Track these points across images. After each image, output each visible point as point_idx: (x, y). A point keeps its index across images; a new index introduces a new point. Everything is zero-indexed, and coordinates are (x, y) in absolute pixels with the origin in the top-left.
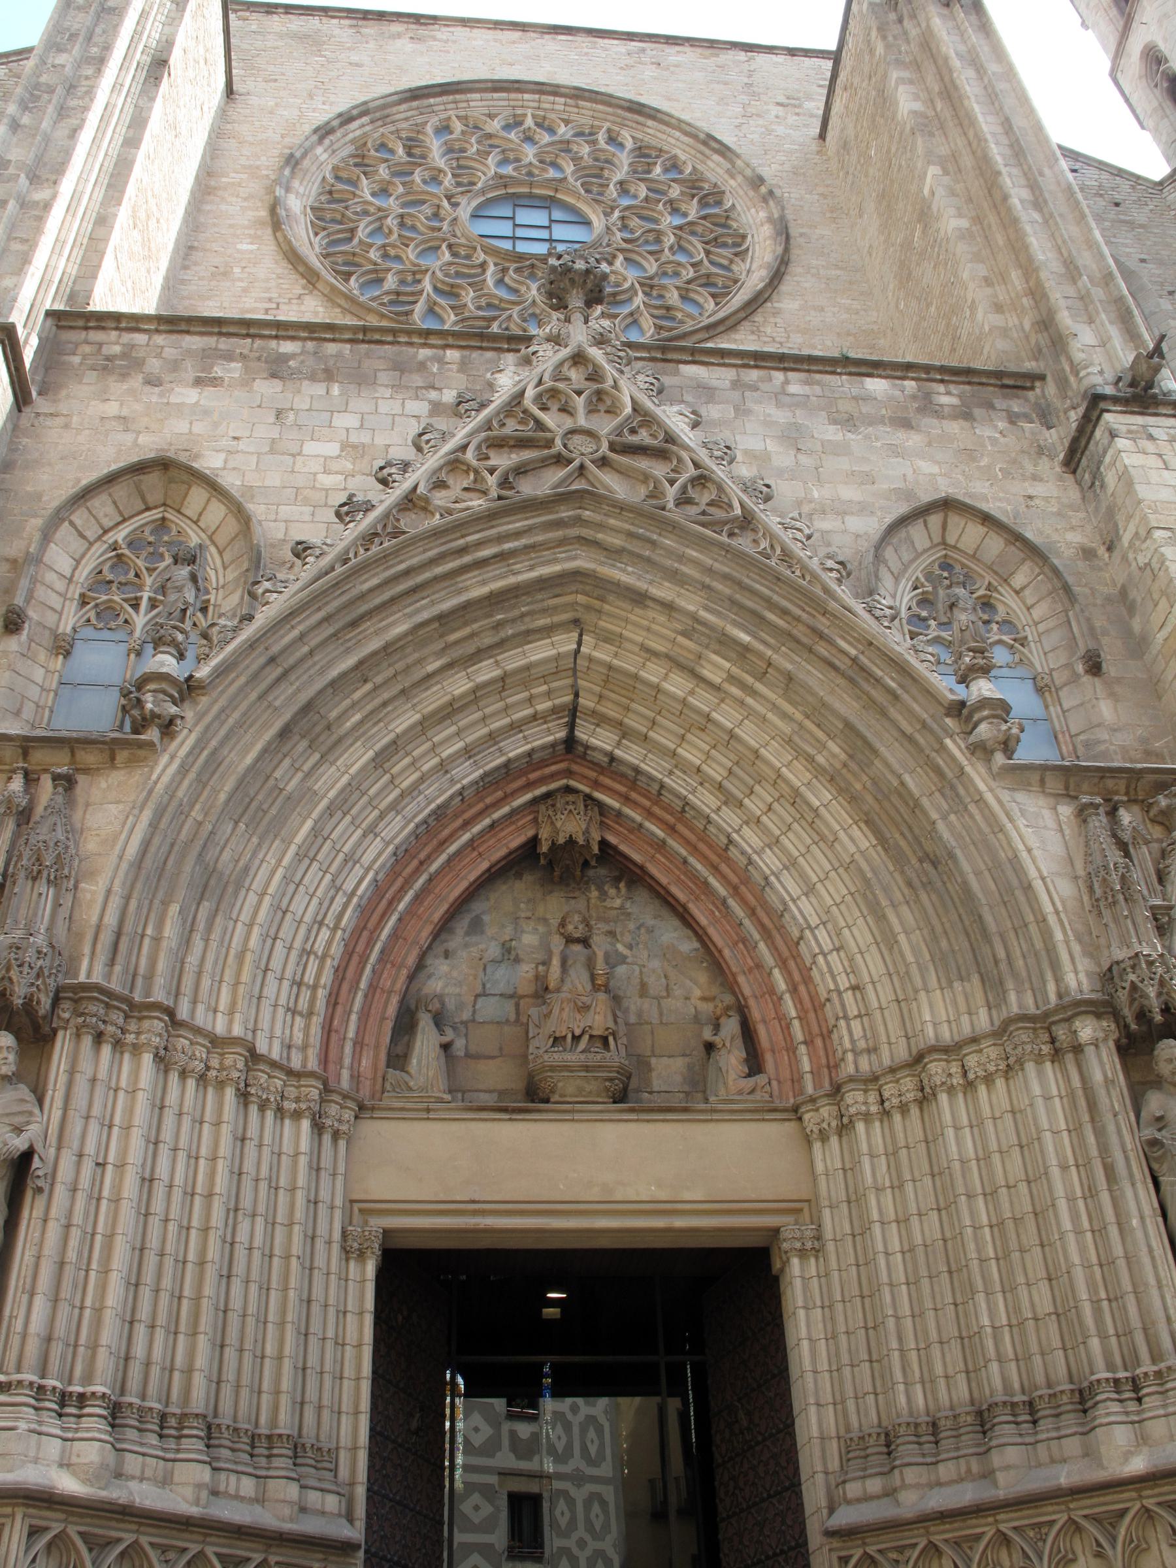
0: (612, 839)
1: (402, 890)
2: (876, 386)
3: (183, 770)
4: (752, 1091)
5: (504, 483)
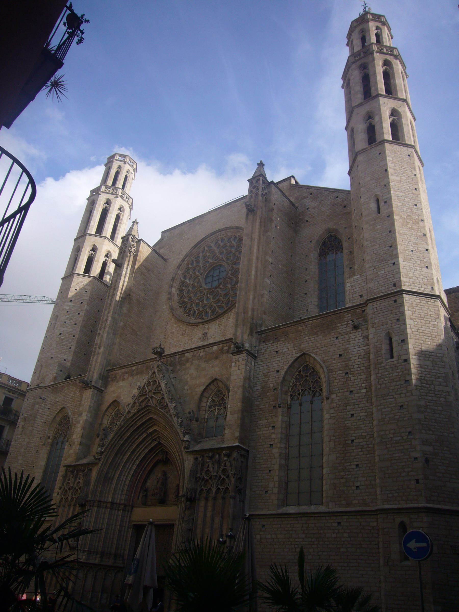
0: (168, 457)
1: (141, 471)
2: (215, 348)
3: (102, 464)
4: (175, 501)
5: (140, 405)
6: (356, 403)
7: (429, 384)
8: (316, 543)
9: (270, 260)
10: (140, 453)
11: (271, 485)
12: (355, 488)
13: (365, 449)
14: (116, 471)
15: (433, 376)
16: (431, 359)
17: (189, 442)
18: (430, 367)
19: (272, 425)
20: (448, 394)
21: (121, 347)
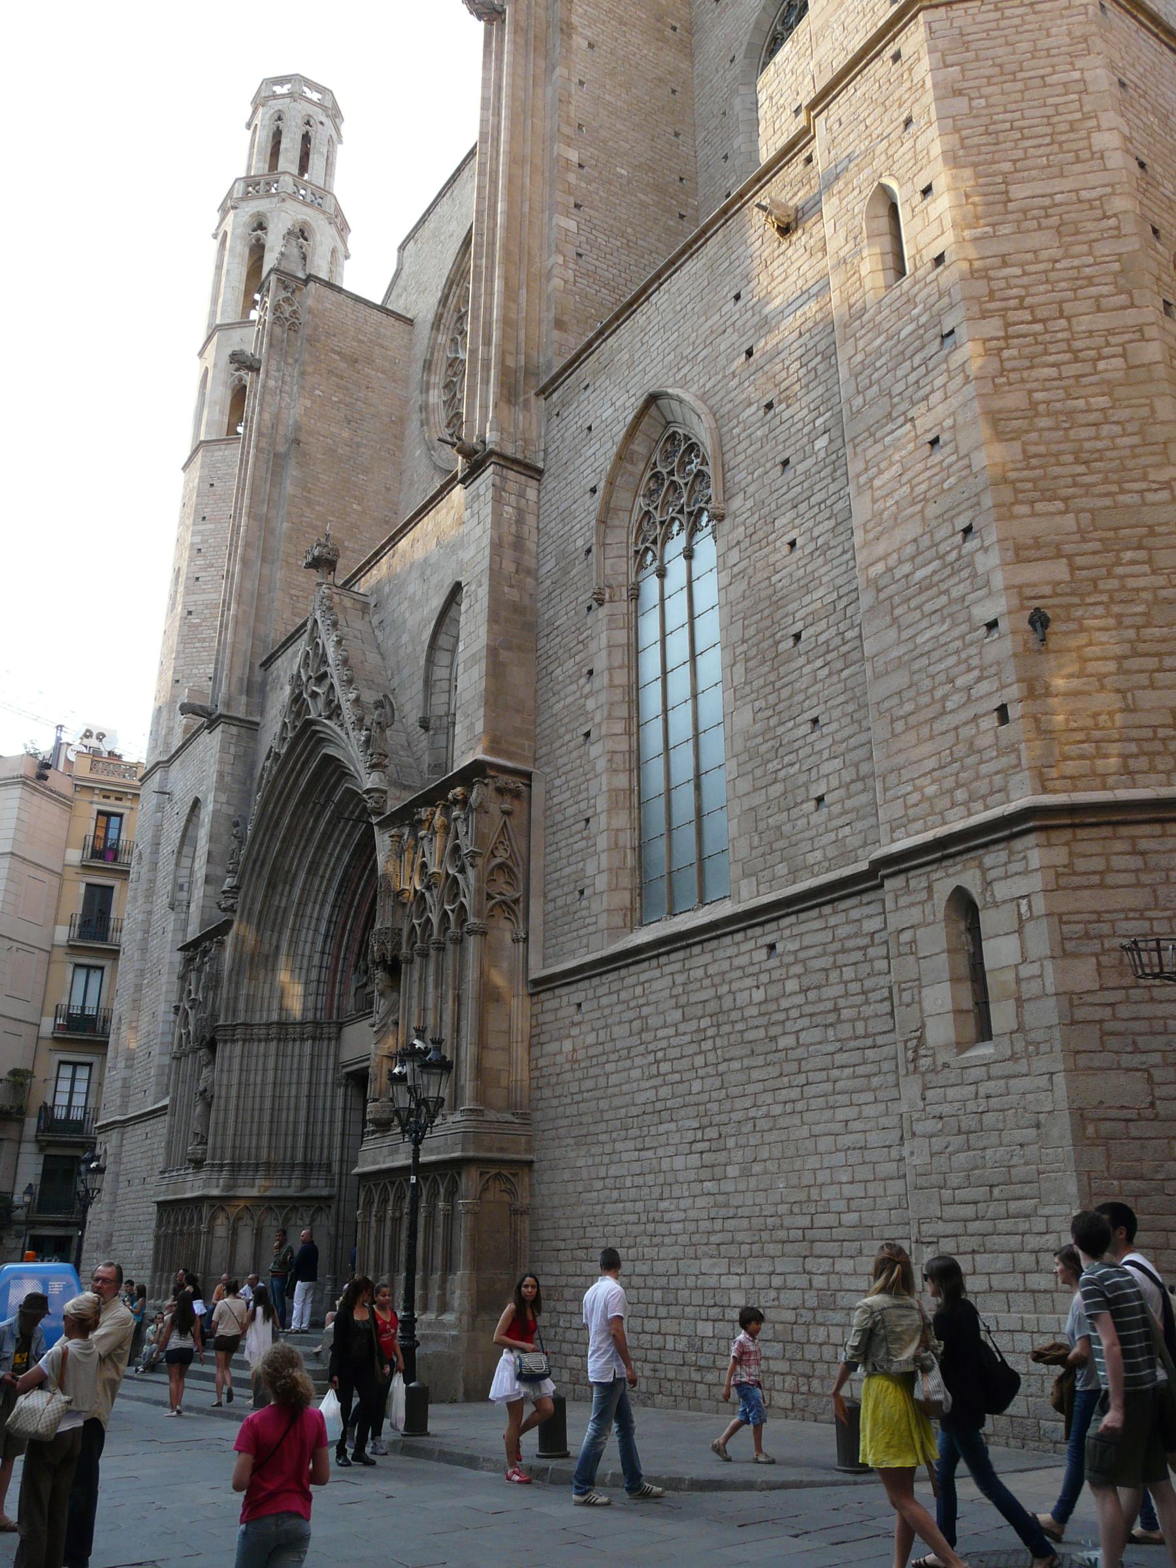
6: (801, 498)
7: (1043, 321)
8: (710, 1032)
9: (574, 156)
10: (334, 869)
11: (591, 869)
12: (812, 804)
13: (834, 654)
14: (280, 933)
15: (1063, 285)
16: (1054, 221)
17: (385, 792)
18: (1044, 255)
19: (585, 671)
20: (1137, 336)
21: (293, 592)
